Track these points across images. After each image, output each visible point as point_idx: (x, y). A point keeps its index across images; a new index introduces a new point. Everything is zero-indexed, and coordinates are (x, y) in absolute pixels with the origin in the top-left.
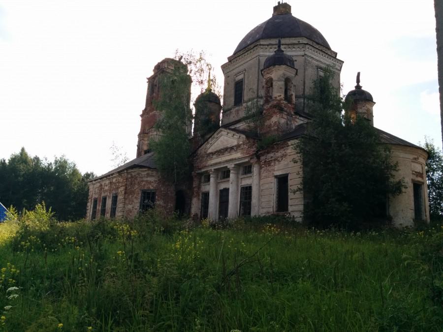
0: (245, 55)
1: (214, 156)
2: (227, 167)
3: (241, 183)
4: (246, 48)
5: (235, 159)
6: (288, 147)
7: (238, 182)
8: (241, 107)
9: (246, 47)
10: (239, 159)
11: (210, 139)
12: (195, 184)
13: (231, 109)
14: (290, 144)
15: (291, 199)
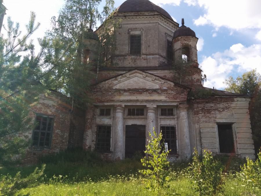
0: (146, 17)
1: (125, 94)
2: (146, 106)
3: (160, 123)
4: (139, 13)
5: (157, 101)
6: (233, 102)
7: (157, 121)
8: (139, 57)
9: (140, 11)
10: (161, 101)
11: (120, 77)
12: (89, 116)
13: (126, 56)
14: (235, 100)
15: (239, 144)
